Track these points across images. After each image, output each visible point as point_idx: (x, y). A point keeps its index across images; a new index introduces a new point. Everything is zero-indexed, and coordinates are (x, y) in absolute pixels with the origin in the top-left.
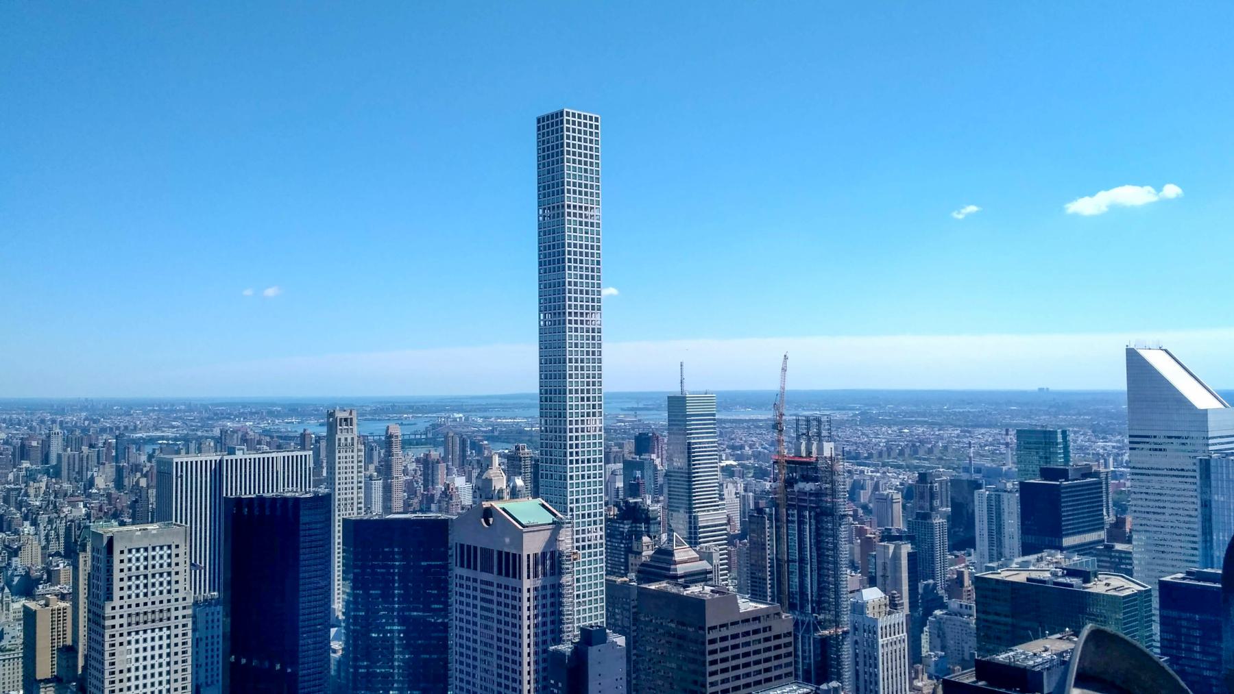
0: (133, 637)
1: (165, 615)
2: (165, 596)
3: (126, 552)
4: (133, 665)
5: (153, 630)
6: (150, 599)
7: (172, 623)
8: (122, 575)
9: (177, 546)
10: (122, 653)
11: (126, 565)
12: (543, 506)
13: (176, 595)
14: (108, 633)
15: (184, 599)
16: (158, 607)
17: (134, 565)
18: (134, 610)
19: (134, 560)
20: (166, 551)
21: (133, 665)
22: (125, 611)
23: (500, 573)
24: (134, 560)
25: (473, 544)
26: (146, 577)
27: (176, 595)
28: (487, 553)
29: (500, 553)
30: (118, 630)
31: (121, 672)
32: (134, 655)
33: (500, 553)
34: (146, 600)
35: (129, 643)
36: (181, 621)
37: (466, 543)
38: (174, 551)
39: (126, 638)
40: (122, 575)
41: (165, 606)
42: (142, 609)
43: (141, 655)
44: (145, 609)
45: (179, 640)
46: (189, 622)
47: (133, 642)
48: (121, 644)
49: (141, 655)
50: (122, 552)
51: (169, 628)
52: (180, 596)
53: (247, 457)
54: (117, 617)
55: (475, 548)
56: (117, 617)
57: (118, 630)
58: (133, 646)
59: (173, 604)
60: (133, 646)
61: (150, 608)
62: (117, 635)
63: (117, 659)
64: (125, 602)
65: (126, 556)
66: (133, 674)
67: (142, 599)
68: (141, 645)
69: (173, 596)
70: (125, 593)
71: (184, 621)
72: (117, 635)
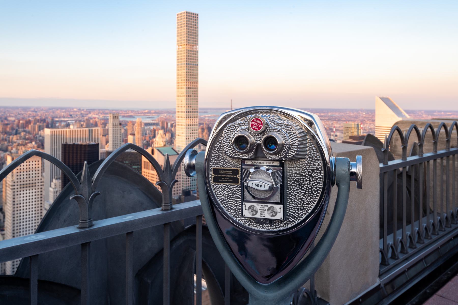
0: (22, 192)
1: (34, 185)
2: (34, 179)
6: (28, 179)
7: (37, 187)
10: (17, 198)
15: (41, 179)
16: (31, 182)
18: (22, 183)
22: (19, 183)
31: (17, 204)
32: (22, 199)
38: (37, 163)
39: (19, 193)
41: (34, 182)
42: (25, 183)
43: (25, 198)
49: (25, 198)
51: (35, 189)
58: (22, 196)
59: (37, 181)
61: (28, 182)
67: (25, 179)
69: (37, 178)
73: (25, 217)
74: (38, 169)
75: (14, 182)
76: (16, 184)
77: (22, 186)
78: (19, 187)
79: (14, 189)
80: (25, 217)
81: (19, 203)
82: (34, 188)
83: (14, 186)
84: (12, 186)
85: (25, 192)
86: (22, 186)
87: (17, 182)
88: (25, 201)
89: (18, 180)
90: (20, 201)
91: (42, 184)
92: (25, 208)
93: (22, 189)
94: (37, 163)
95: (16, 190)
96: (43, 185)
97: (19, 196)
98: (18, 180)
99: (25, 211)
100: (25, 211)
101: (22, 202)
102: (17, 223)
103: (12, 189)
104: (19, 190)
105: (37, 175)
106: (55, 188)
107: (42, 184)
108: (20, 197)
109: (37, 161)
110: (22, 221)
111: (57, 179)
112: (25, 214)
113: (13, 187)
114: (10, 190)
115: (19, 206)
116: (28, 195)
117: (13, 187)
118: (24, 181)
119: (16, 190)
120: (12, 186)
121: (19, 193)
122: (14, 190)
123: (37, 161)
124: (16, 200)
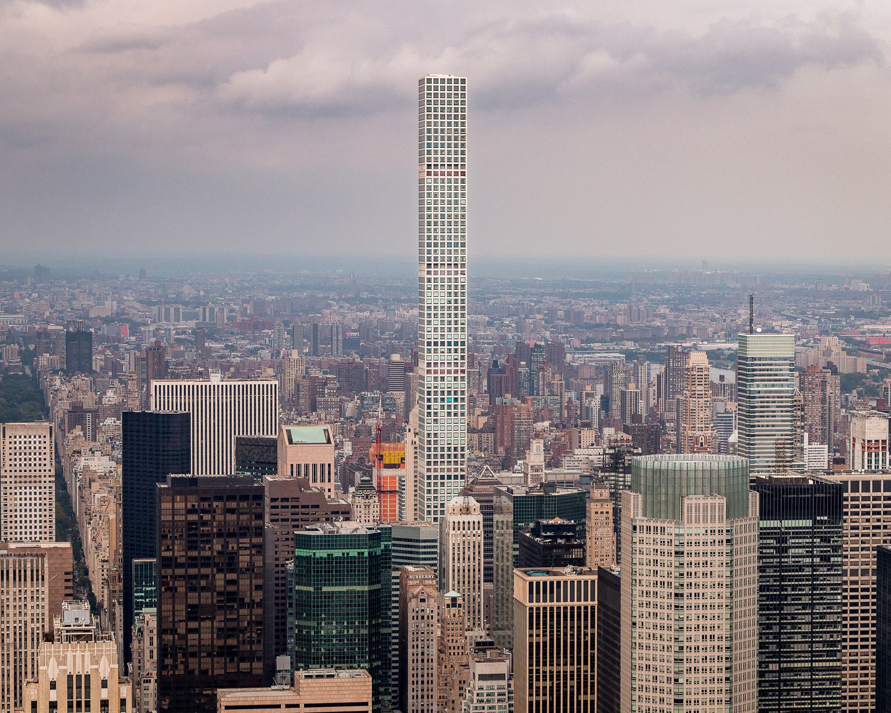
4: (18, 508)
5: (21, 488)
13: (45, 468)
14: (3, 486)
17: (18, 445)
18: (18, 473)
21: (18, 508)
22: (13, 474)
26: (25, 454)
27: (45, 468)
30: (8, 485)
32: (18, 502)
34: (26, 468)
35: (16, 494)
36: (48, 485)
38: (42, 439)
39: (13, 491)
40: (11, 451)
41: (38, 473)
43: (23, 502)
44: (25, 474)
45: (47, 496)
46: (53, 485)
52: (48, 468)
57: (8, 485)
58: (18, 496)
63: (9, 502)
64: (13, 468)
65: (13, 440)
66: (18, 513)
67: (23, 468)
68: (23, 496)
70: (13, 462)
71: (50, 485)
74: (45, 451)
81: (13, 508)
82: (38, 485)
88: (23, 508)
89: (11, 468)
90: (16, 505)
93: (18, 485)
98: (11, 468)
100: (23, 524)
104: (13, 485)
105: (43, 462)
108: (16, 499)
116: (28, 496)
121: (13, 491)
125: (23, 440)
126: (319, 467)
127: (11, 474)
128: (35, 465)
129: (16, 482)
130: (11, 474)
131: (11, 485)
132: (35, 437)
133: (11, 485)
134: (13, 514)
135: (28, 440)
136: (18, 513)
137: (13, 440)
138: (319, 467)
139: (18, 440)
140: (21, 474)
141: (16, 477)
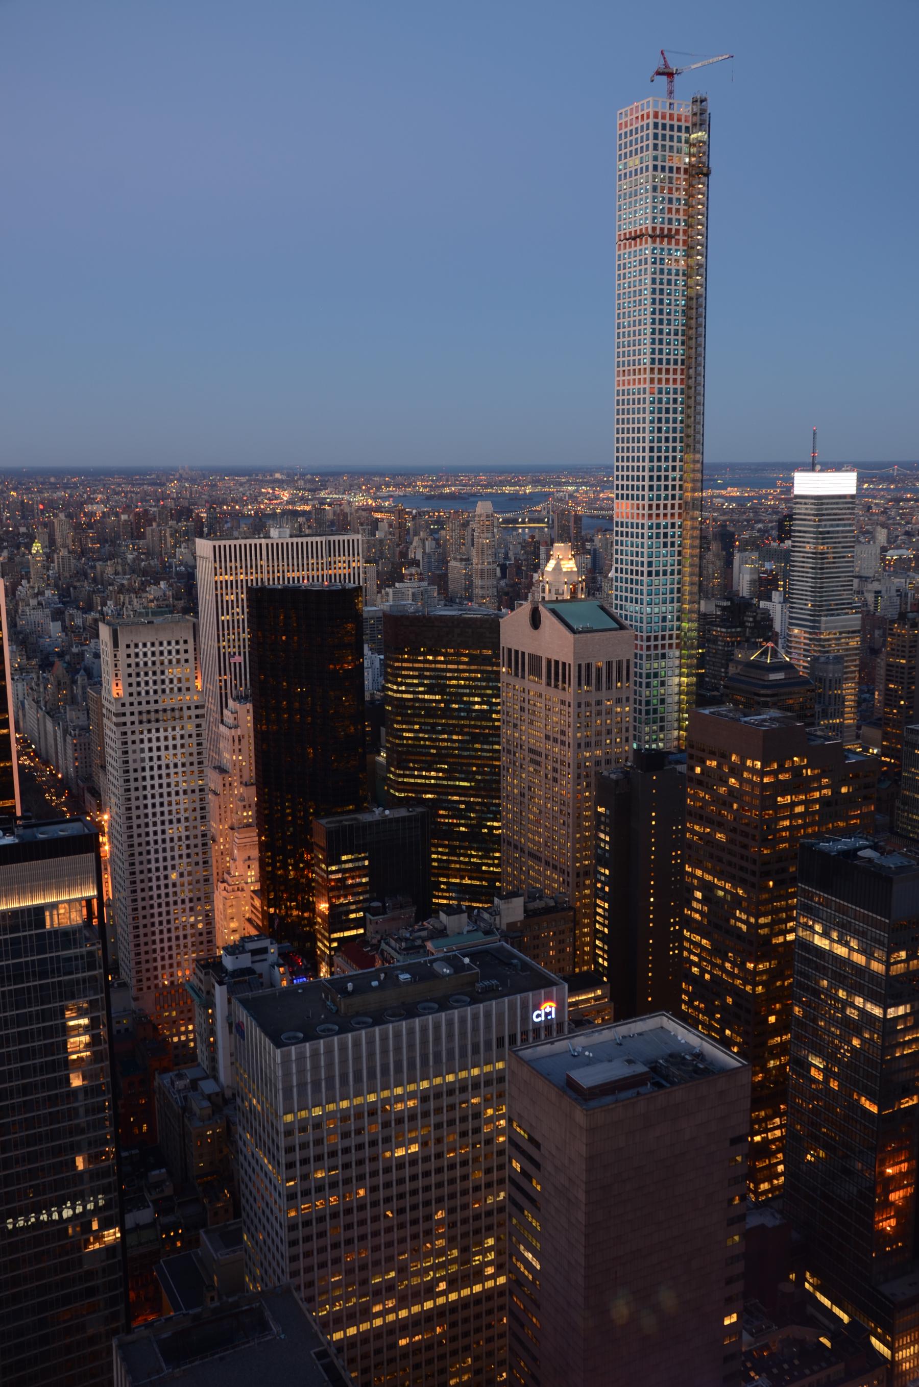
0: (146, 736)
3: (132, 646)
8: (130, 670)
9: (186, 642)
11: (132, 660)
12: (602, 608)
18: (144, 707)
19: (141, 654)
20: (173, 647)
22: (136, 709)
23: (549, 684)
24: (141, 654)
25: (520, 649)
28: (535, 660)
29: (549, 661)
32: (147, 755)
33: (549, 661)
37: (514, 647)
38: (181, 647)
39: (137, 737)
40: (130, 670)
47: (146, 741)
48: (134, 742)
50: (128, 646)
53: (290, 540)
54: (128, 714)
55: (523, 653)
56: (128, 714)
58: (146, 745)
60: (146, 745)
62: (129, 733)
65: (132, 651)
72: (129, 733)
73: (158, 809)
75: (123, 705)
76: (128, 709)
77: (145, 717)
78: (135, 718)
79: (125, 724)
80: (158, 809)
81: (138, 766)
83: (124, 714)
84: (117, 715)
85: (154, 735)
86: (145, 717)
87: (132, 704)
89: (132, 699)
90: (143, 760)
91: (199, 712)
92: (156, 782)
93: (146, 726)
94: (181, 647)
95: (128, 728)
96: (203, 716)
97: (138, 746)
98: (132, 699)
99: (157, 791)
100: (157, 791)
101: (147, 764)
102: (139, 826)
103: (116, 724)
104: (137, 728)
106: (236, 727)
107: (199, 712)
108: (142, 751)
109: (181, 642)
110: (150, 820)
111: (238, 698)
112: (158, 800)
113: (122, 719)
114: (114, 728)
115: (139, 775)
117: (122, 719)
118: (148, 702)
119: (128, 728)
120: (117, 715)
121: (137, 737)
122: (123, 729)
123: (181, 642)
124: (131, 757)
125: (149, 649)
126: (614, 665)
127: (132, 709)
128: (147, 693)
129: (141, 722)
130: (132, 709)
131: (133, 728)
132: (169, 643)
133: (133, 728)
134: (139, 775)
135: (157, 649)
136: (147, 774)
137: (132, 651)
138: (614, 665)
139: (141, 650)
140: (149, 707)
141: (140, 713)
